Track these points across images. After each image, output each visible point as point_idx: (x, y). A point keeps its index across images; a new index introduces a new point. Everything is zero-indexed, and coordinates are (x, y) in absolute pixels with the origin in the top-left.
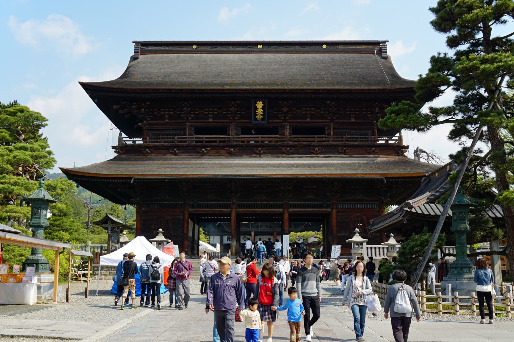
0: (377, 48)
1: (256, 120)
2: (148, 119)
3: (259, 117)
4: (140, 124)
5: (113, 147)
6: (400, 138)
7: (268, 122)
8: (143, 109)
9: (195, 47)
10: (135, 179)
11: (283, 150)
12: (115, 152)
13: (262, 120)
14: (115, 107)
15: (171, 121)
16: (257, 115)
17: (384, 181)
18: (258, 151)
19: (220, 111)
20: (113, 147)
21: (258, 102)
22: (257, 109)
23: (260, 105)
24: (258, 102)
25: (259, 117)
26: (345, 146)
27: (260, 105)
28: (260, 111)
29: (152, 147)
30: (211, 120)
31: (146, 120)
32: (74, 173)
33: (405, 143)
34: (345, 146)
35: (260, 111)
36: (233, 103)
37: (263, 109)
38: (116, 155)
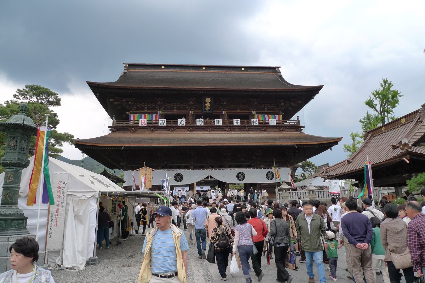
0: (275, 70)
1: (205, 110)
2: (133, 109)
3: (208, 108)
4: (127, 113)
5: (109, 127)
6: (298, 121)
7: (213, 112)
8: (130, 102)
9: (163, 67)
10: (125, 147)
11: (225, 128)
12: (110, 130)
13: (209, 110)
14: (111, 100)
15: (148, 111)
16: (206, 107)
17: (295, 148)
18: (208, 130)
19: (181, 105)
20: (109, 127)
21: (207, 98)
22: (206, 103)
23: (208, 100)
24: (207, 98)
25: (208, 108)
26: (265, 127)
27: (208, 100)
28: (208, 105)
29: (136, 127)
30: (175, 110)
31: (131, 110)
32: (81, 143)
33: (301, 124)
34: (265, 127)
35: (208, 105)
36: (191, 99)
37: (210, 103)
38: (111, 132)
